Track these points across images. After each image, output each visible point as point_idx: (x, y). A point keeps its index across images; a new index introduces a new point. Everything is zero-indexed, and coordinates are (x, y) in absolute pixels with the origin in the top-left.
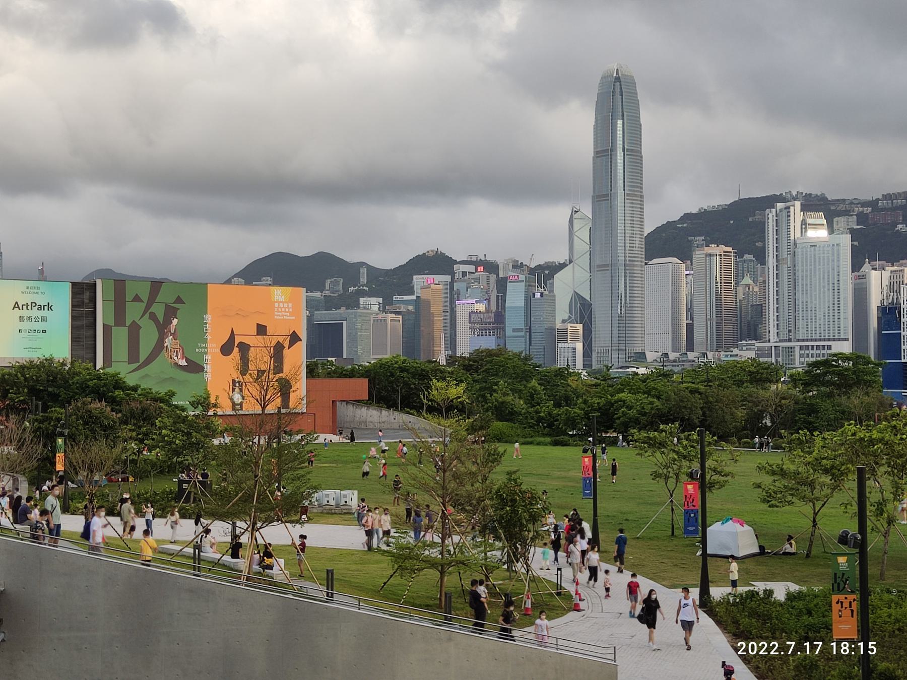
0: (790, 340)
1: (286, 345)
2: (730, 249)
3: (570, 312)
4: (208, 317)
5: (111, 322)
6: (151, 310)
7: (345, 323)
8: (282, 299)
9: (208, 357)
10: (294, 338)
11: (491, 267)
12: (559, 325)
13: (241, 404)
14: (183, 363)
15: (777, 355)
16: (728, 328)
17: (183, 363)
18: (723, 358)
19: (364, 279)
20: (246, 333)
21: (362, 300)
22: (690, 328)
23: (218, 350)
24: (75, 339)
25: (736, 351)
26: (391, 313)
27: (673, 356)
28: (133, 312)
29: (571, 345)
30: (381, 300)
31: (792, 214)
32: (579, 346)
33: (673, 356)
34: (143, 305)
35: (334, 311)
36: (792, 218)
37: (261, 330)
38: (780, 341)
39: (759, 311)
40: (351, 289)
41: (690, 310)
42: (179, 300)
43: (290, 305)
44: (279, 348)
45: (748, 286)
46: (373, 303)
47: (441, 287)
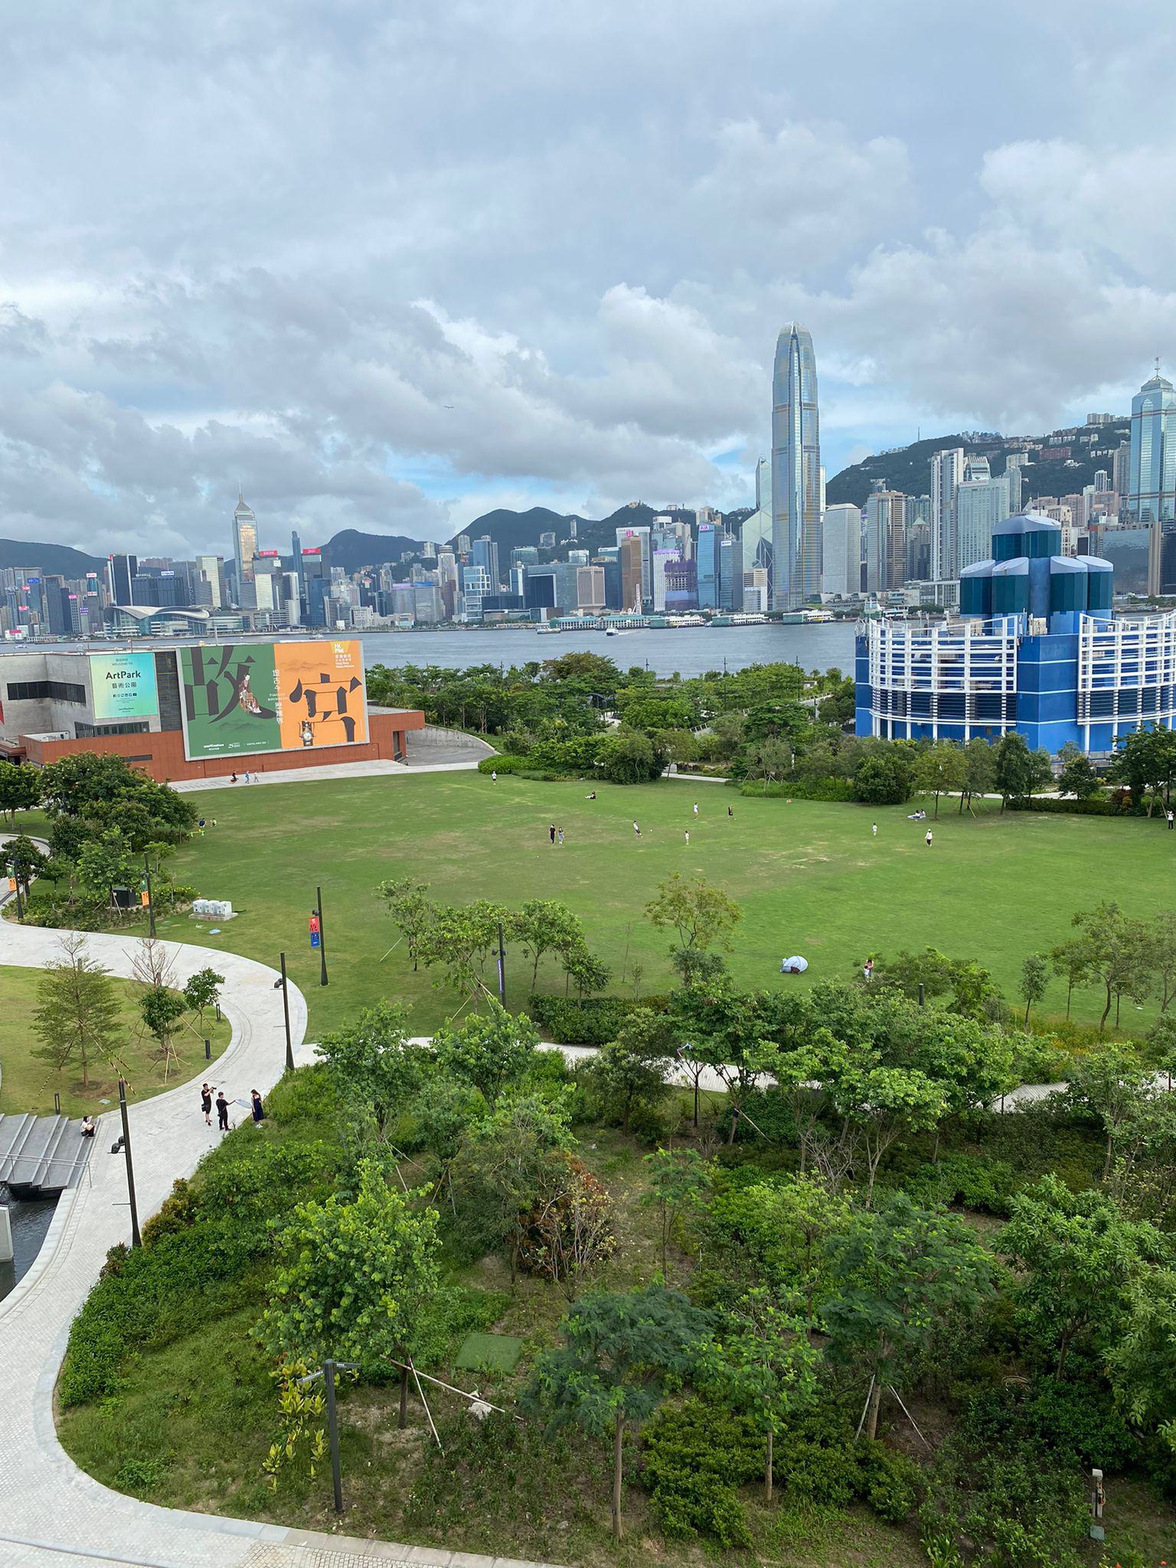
0: (951, 579)
1: (348, 688)
2: (901, 494)
3: (758, 557)
5: (192, 683)
8: (342, 651)
9: (279, 705)
10: (355, 683)
11: (687, 517)
12: (745, 571)
13: (311, 741)
14: (258, 711)
15: (940, 593)
16: (897, 568)
17: (258, 711)
18: (890, 597)
22: (864, 568)
24: (162, 699)
25: (902, 591)
26: (595, 564)
27: (845, 596)
28: (210, 673)
29: (756, 589)
30: (587, 552)
31: (955, 460)
32: (764, 590)
33: (845, 596)
34: (217, 668)
35: (545, 565)
36: (955, 464)
38: (943, 580)
39: (926, 548)
40: (563, 542)
41: (864, 551)
44: (341, 693)
45: (920, 526)
47: (641, 538)
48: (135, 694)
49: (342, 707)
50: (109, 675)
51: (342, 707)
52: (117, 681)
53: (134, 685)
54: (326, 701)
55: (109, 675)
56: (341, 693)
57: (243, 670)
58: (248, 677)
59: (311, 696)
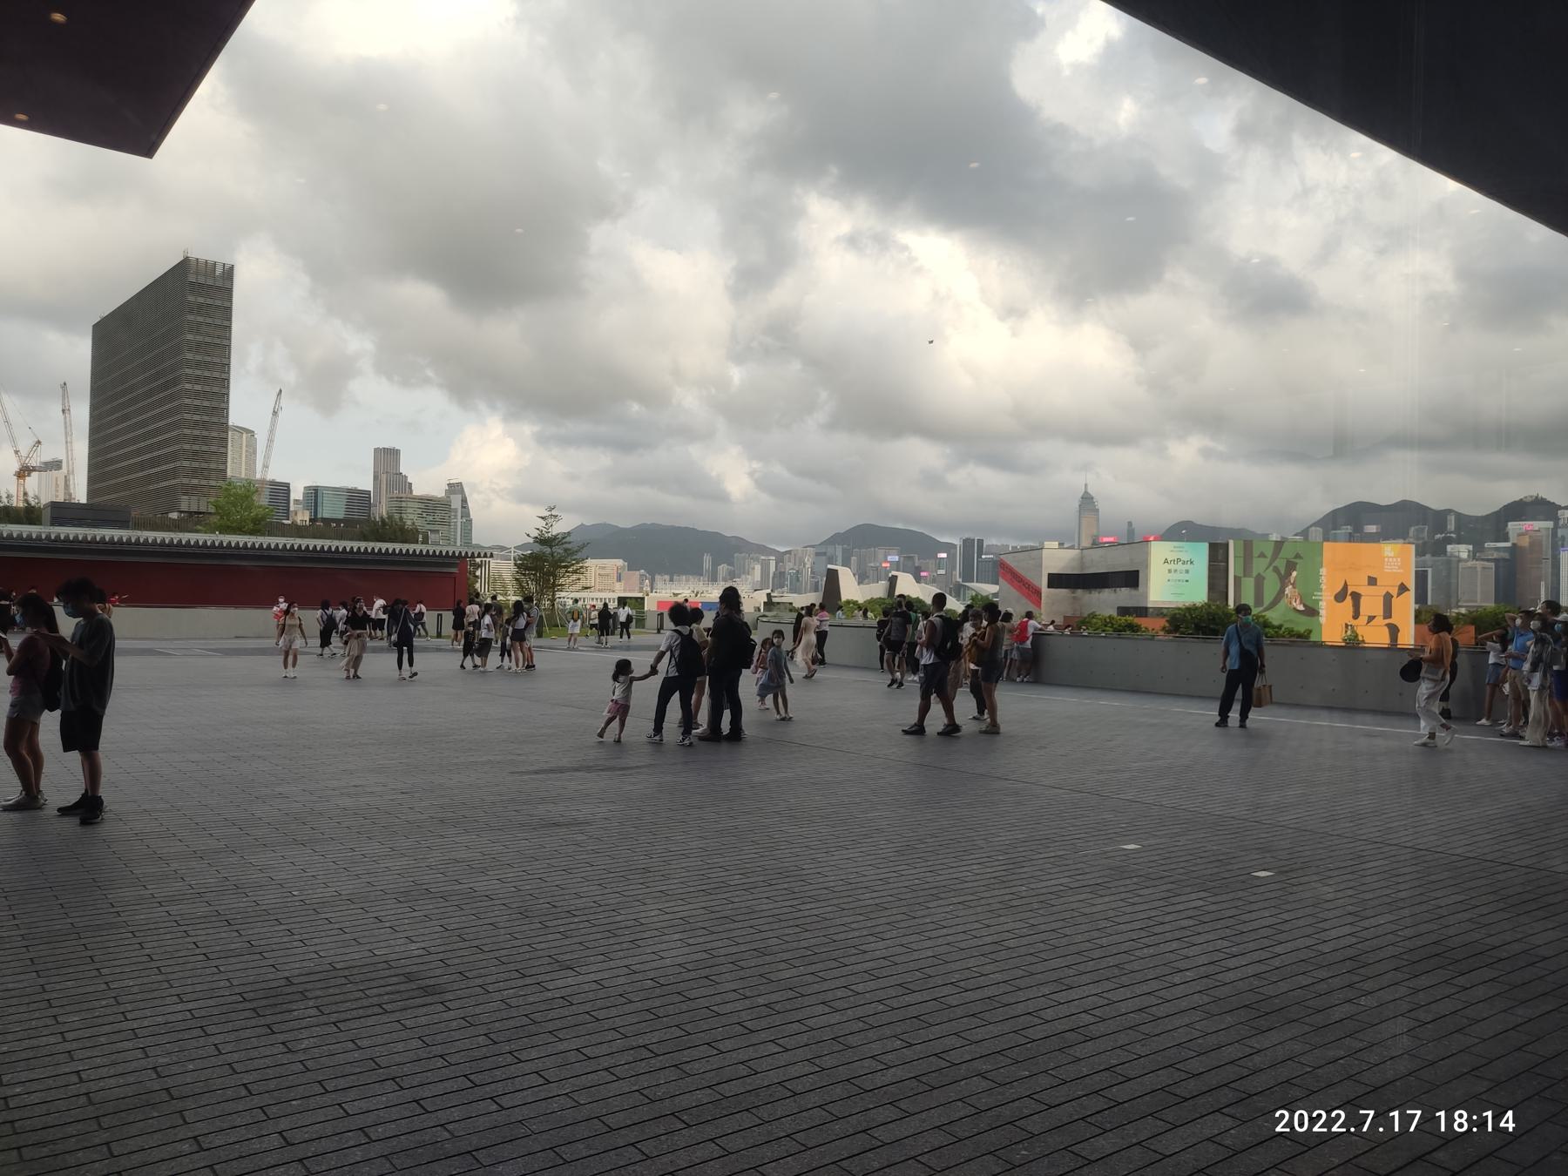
1: (1395, 595)
4: (1323, 571)
6: (1274, 565)
7: (1430, 570)
17: (1301, 608)
19: (1451, 526)
20: (1358, 584)
21: (1449, 548)
23: (1333, 598)
24: (1212, 587)
28: (1259, 566)
37: (1372, 581)
42: (1298, 556)
43: (1399, 560)
46: (1463, 551)
48: (1187, 581)
49: (1388, 613)
50: (1166, 561)
51: (1388, 613)
52: (1172, 566)
53: (1187, 572)
54: (1371, 604)
55: (1166, 561)
56: (1388, 599)
57: (1291, 566)
58: (1294, 574)
59: (1356, 597)
